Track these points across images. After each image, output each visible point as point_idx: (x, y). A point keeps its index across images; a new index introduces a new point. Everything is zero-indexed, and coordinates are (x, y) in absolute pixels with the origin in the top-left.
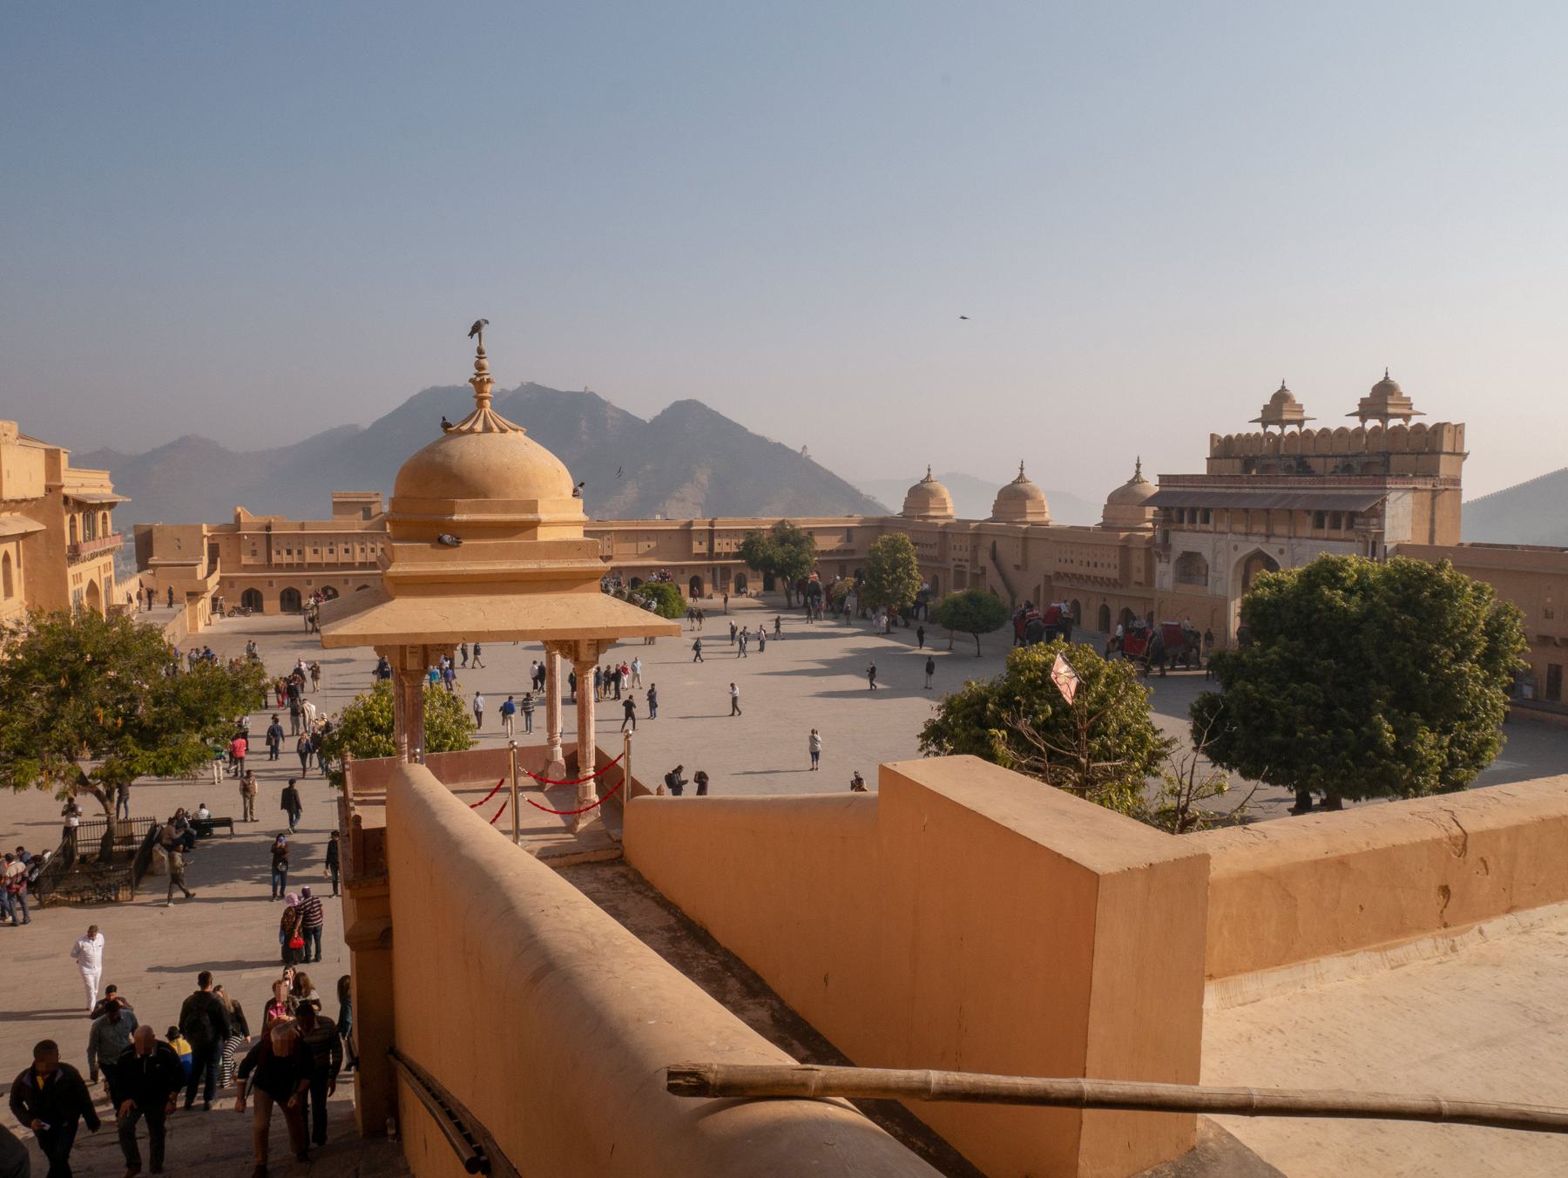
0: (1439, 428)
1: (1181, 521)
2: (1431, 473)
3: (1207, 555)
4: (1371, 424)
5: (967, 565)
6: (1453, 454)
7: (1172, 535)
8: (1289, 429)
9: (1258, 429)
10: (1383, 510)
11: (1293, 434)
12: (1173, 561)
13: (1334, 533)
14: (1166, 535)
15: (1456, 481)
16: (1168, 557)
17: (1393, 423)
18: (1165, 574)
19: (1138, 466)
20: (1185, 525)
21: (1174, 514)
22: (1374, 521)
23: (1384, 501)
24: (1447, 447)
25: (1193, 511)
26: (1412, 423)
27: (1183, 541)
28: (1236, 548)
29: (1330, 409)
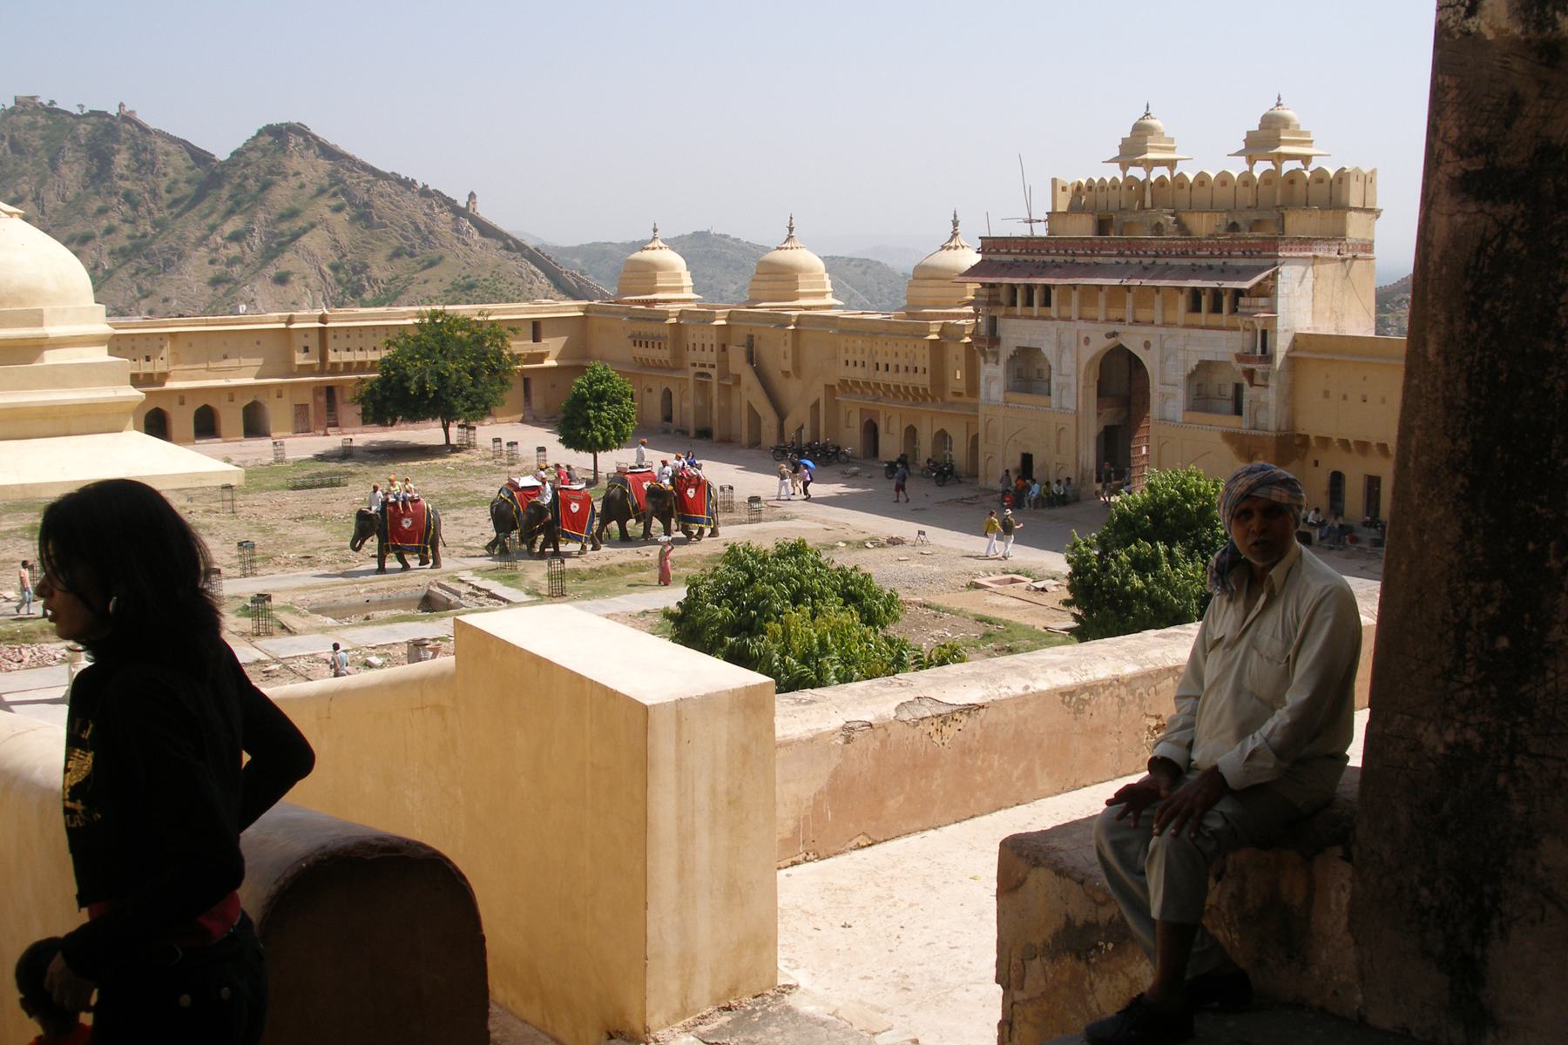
0: (1342, 176)
1: (1014, 304)
2: (1338, 236)
3: (1048, 351)
4: (1261, 168)
5: (714, 372)
6: (1364, 210)
7: (1001, 323)
8: (1157, 172)
9: (1113, 173)
10: (1275, 287)
11: (1161, 180)
12: (1003, 359)
13: (1214, 319)
14: (993, 322)
15: (1368, 247)
16: (996, 354)
17: (1288, 166)
18: (993, 376)
19: (955, 224)
20: (1019, 309)
21: (1004, 297)
22: (1262, 301)
23: (1275, 274)
24: (1355, 201)
26: (1312, 167)
27: (1018, 332)
28: (1087, 340)
29: (1207, 150)
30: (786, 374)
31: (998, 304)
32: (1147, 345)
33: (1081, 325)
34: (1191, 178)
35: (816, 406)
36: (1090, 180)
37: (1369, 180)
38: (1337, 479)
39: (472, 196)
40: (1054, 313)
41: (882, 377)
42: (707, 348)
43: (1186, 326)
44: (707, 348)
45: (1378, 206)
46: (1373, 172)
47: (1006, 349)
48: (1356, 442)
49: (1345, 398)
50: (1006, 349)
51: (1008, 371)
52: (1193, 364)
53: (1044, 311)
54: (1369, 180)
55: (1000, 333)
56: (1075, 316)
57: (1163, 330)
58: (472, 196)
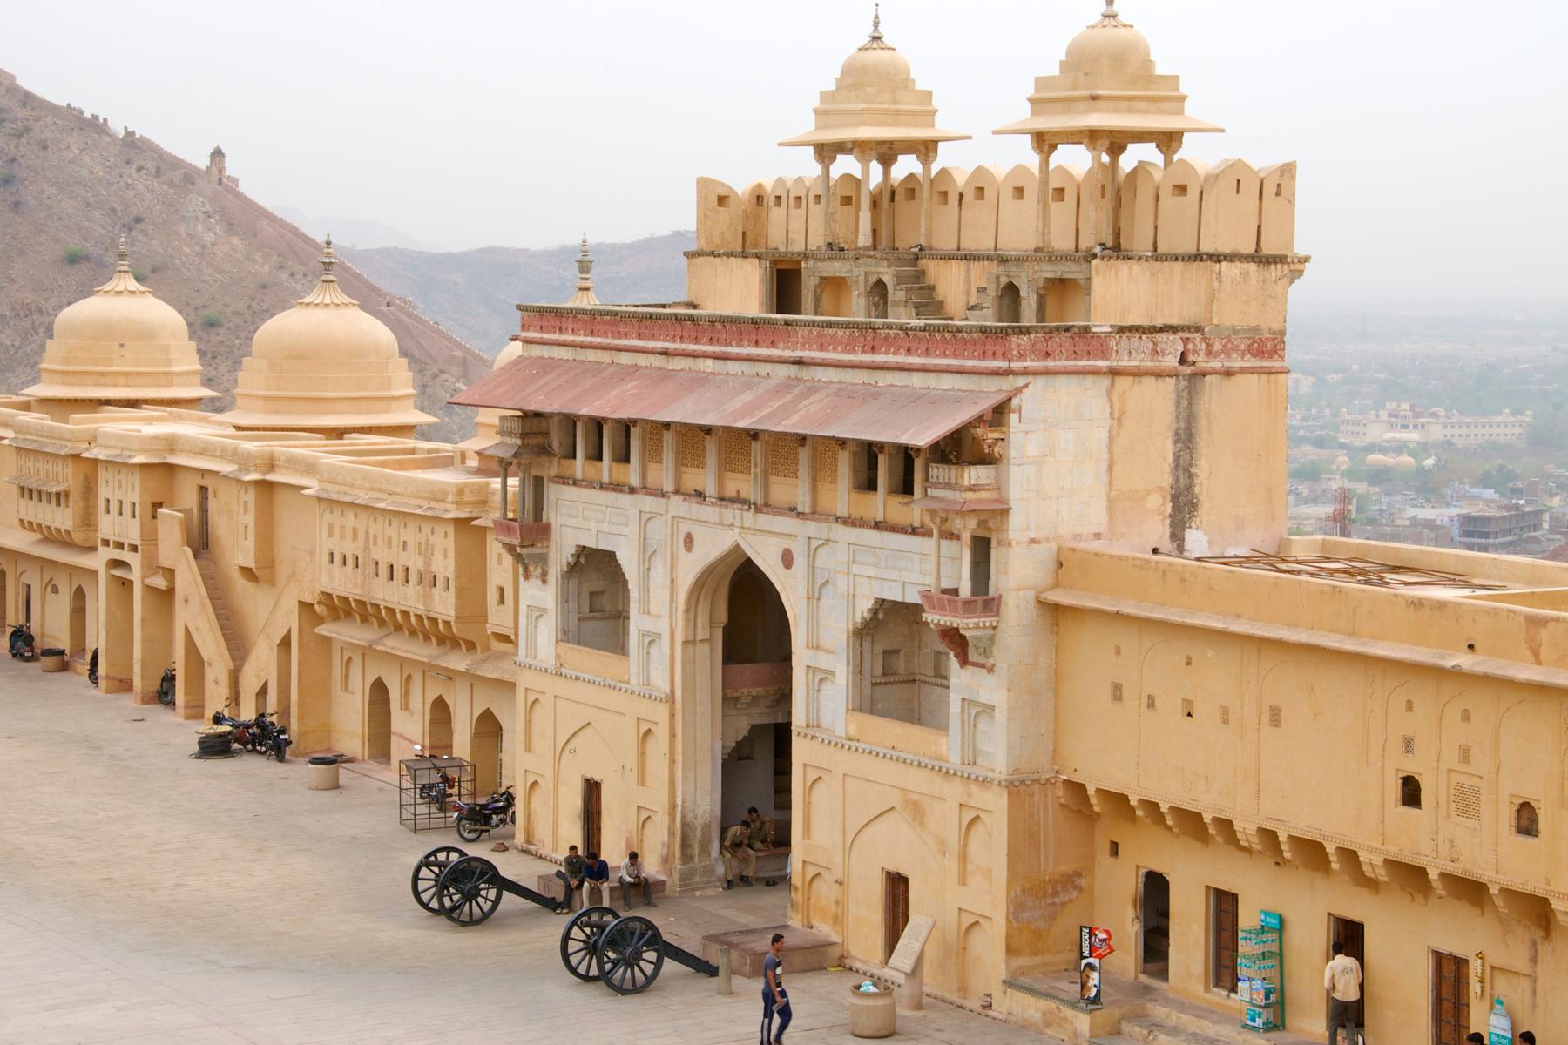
5: (134, 560)
8: (906, 165)
16: (543, 560)
20: (579, 466)
25: (598, 424)
27: (583, 515)
30: (247, 572)
31: (545, 451)
32: (787, 559)
33: (678, 505)
34: (961, 180)
35: (285, 643)
36: (780, 181)
37: (1275, 187)
38: (1155, 890)
39: (218, 154)
40: (634, 481)
41: (386, 594)
42: (127, 509)
43: (849, 522)
44: (127, 509)
45: (1300, 249)
46: (1288, 170)
47: (560, 552)
48: (1175, 810)
49: (1151, 703)
50: (560, 552)
51: (564, 599)
52: (864, 607)
54: (1275, 187)
55: (551, 515)
56: (668, 486)
57: (811, 528)
58: (218, 154)
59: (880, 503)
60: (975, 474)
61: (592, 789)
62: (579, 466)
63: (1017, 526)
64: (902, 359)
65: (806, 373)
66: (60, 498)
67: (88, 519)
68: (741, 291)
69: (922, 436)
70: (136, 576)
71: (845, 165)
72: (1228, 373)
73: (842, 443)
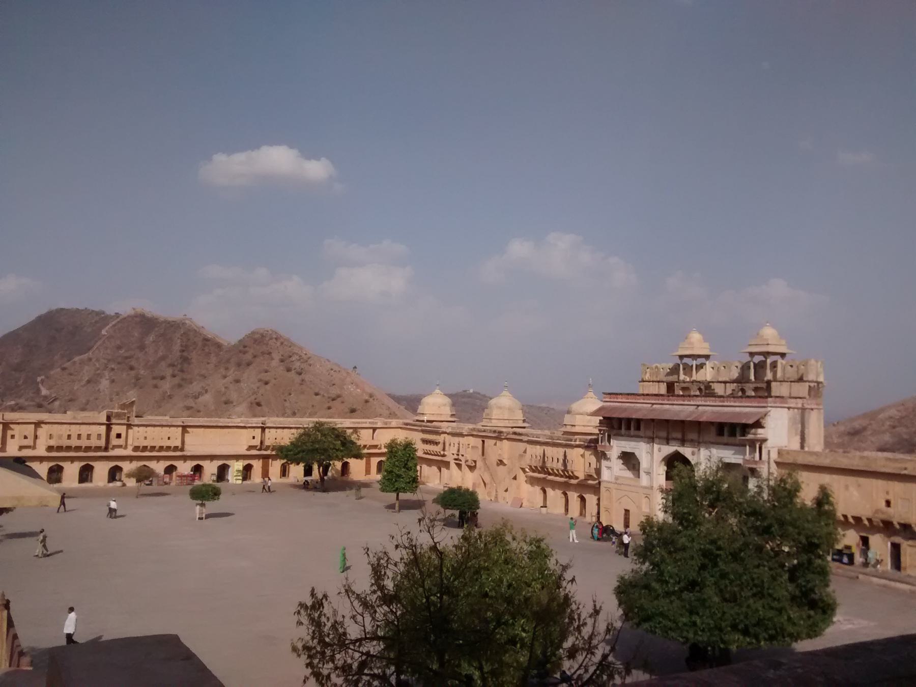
20: (623, 431)
53: (637, 433)
59: (726, 438)
60: (760, 431)
61: (627, 512)
62: (623, 431)
63: (769, 444)
64: (732, 404)
65: (700, 408)
66: (437, 443)
67: (444, 450)
68: (663, 389)
69: (751, 422)
70: (463, 463)
71: (686, 360)
72: (812, 409)
73: (712, 423)
